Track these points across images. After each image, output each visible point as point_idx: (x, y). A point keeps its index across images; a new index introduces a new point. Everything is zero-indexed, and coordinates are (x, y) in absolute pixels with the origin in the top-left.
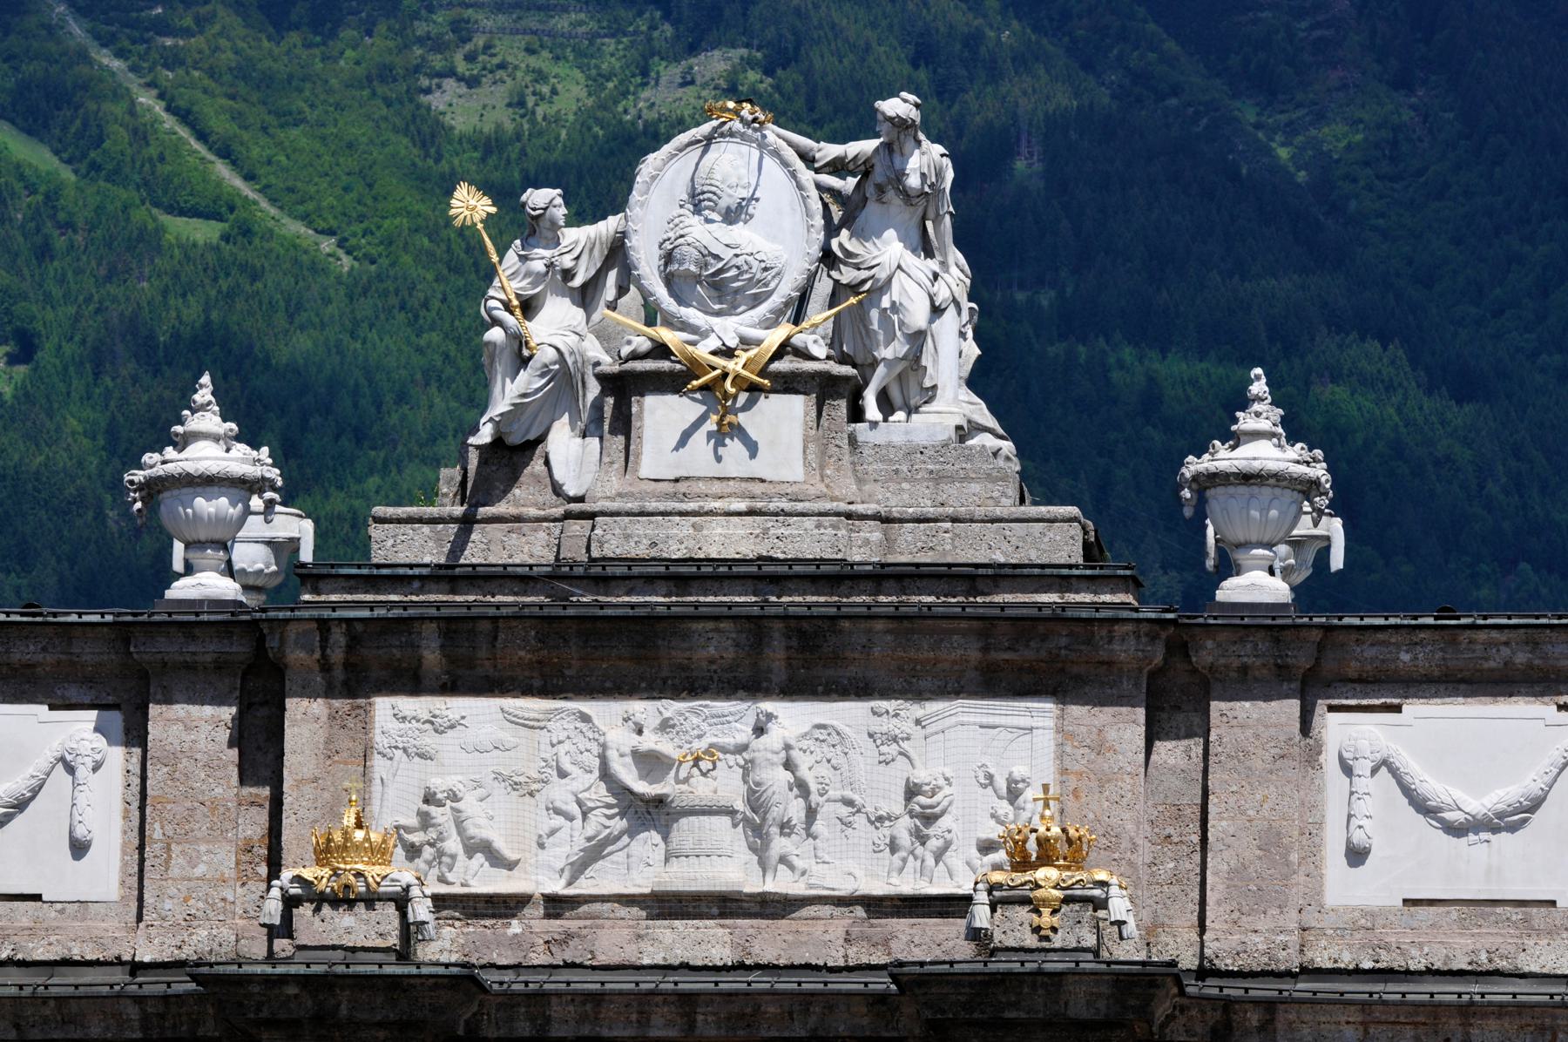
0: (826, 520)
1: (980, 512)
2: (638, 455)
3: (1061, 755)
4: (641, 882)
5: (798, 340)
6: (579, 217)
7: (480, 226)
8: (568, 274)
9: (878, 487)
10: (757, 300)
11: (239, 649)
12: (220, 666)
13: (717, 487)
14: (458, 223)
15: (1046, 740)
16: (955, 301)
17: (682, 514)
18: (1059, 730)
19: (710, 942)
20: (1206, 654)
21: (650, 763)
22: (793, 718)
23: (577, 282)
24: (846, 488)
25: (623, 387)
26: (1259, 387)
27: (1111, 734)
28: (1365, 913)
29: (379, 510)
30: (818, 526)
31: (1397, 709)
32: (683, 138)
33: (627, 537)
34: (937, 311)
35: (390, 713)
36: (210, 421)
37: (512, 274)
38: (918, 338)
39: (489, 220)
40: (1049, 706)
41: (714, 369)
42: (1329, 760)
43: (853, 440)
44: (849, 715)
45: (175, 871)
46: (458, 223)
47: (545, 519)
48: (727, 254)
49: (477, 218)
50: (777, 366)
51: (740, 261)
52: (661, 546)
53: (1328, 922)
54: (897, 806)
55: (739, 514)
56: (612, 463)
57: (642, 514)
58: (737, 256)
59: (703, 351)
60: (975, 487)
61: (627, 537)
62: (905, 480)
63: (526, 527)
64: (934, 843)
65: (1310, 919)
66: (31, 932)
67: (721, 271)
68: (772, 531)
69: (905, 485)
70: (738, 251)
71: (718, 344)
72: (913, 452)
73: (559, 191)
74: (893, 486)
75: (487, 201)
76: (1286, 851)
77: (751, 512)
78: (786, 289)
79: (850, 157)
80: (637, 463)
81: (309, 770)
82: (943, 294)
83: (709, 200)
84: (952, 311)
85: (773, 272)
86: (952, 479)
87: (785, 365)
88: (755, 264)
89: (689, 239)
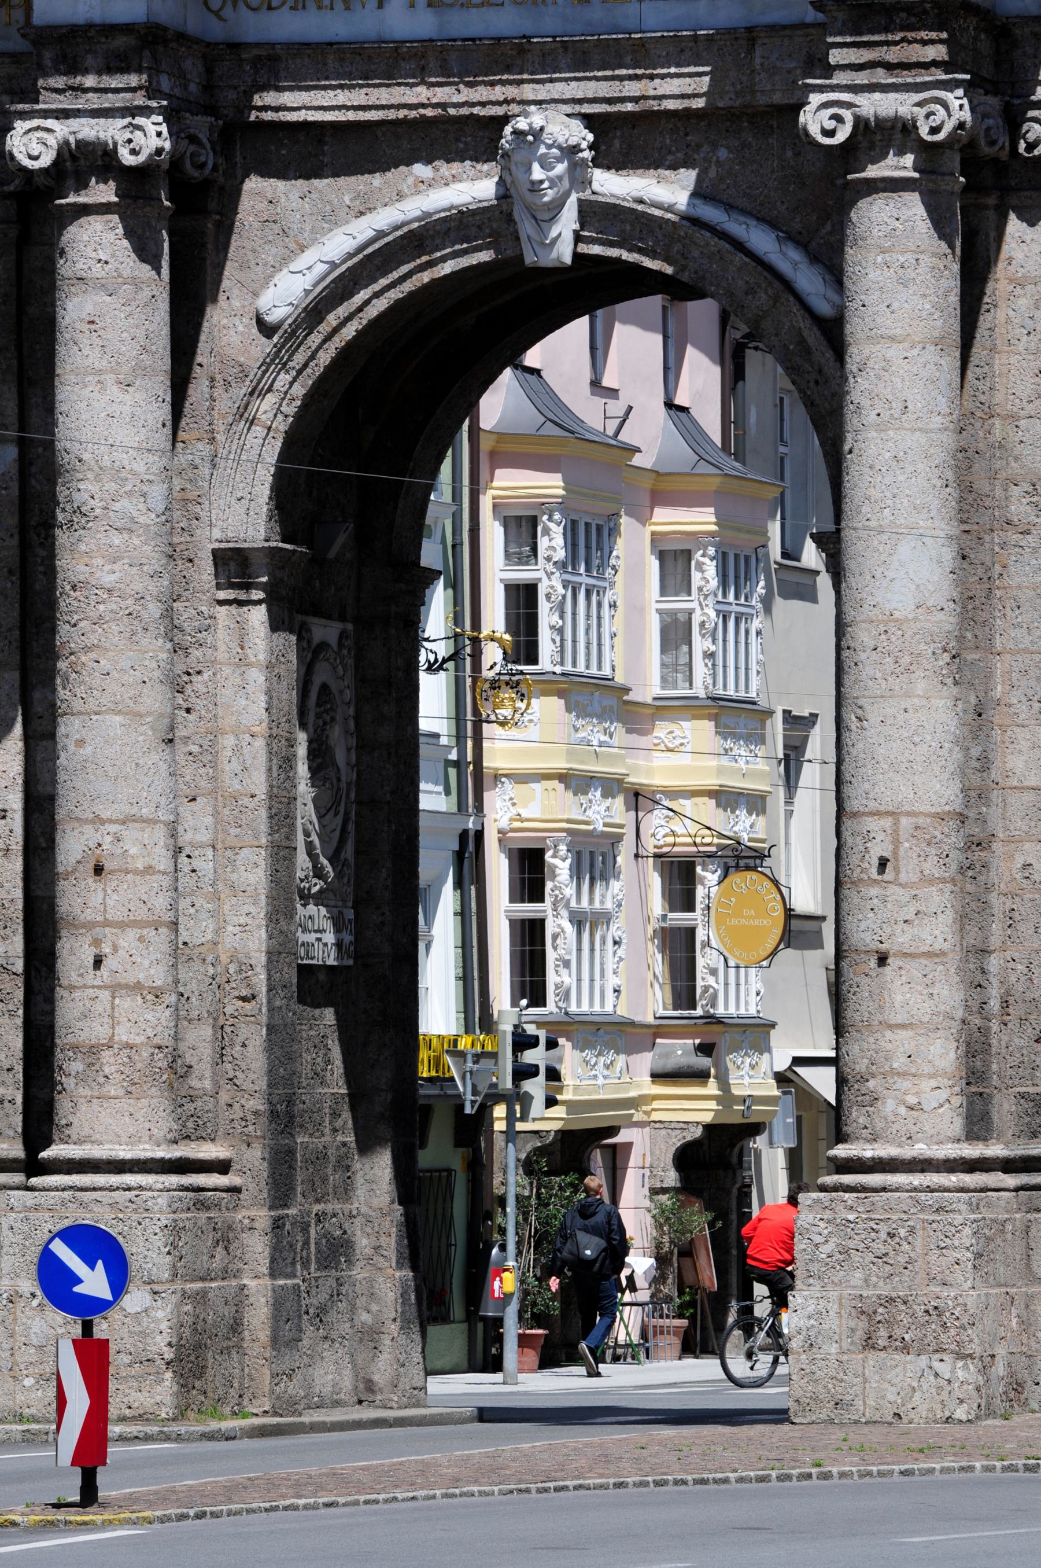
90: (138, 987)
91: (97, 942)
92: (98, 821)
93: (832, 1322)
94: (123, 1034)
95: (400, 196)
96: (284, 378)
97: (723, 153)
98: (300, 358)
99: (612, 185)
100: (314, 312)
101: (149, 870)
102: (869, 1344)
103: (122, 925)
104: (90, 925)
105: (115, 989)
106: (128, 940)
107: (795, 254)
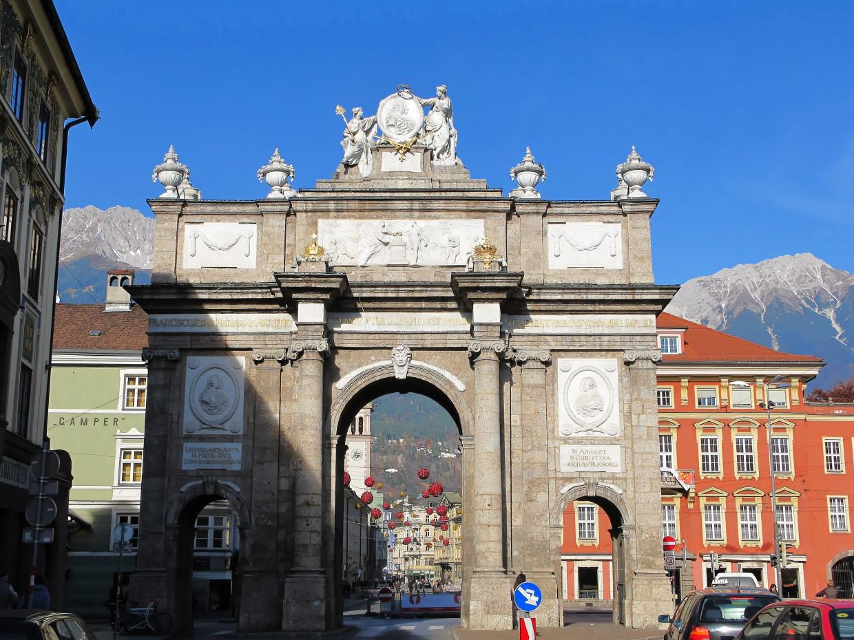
3: (486, 233)
4: (385, 263)
10: (409, 131)
11: (286, 208)
12: (281, 213)
13: (400, 174)
15: (482, 229)
18: (485, 227)
19: (400, 277)
20: (519, 209)
21: (386, 233)
22: (422, 223)
23: (365, 130)
25: (377, 149)
26: (528, 151)
27: (498, 228)
28: (559, 270)
29: (318, 180)
31: (565, 223)
32: (392, 95)
33: (379, 184)
35: (321, 223)
36: (278, 158)
40: (482, 221)
42: (549, 234)
43: (432, 165)
44: (435, 223)
45: (269, 261)
53: (550, 273)
54: (446, 243)
60: (461, 175)
64: (456, 254)
65: (545, 272)
66: (235, 275)
72: (445, 167)
76: (540, 256)
81: (302, 237)
86: (455, 173)
90: (316, 531)
91: (307, 521)
92: (308, 494)
93: (480, 608)
94: (313, 542)
95: (368, 364)
96: (341, 401)
97: (438, 357)
98: (345, 397)
99: (413, 362)
100: (350, 385)
101: (318, 505)
102: (488, 613)
103: (313, 517)
104: (305, 517)
105: (311, 531)
106: (314, 521)
107: (455, 377)
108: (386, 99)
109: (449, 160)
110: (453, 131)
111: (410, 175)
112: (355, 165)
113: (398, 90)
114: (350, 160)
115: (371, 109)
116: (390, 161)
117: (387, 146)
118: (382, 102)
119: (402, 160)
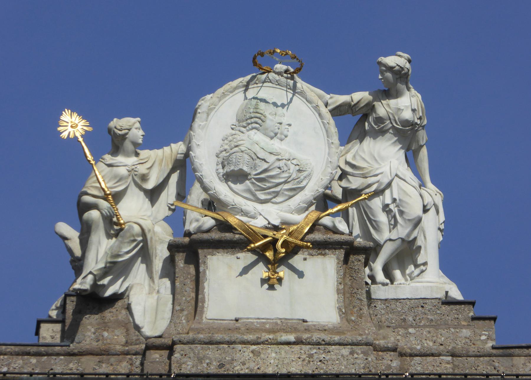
0: (357, 349)
1: (473, 349)
2: (204, 301)
5: (327, 221)
6: (153, 141)
7: (81, 139)
8: (144, 178)
9: (389, 331)
14: (64, 135)
16: (435, 205)
17: (243, 343)
24: (368, 331)
30: (352, 353)
34: (425, 210)
37: (104, 175)
38: (417, 222)
39: (86, 136)
41: (265, 237)
46: (64, 135)
47: (127, 353)
48: (271, 159)
49: (78, 135)
50: (311, 237)
51: (281, 164)
52: (228, 366)
55: (288, 343)
56: (182, 310)
57: (211, 343)
58: (279, 160)
59: (258, 223)
61: (200, 360)
62: (411, 326)
63: (113, 359)
67: (265, 171)
68: (316, 356)
69: (411, 330)
70: (280, 157)
71: (265, 223)
73: (139, 119)
74: (402, 331)
75: (83, 122)
77: (299, 342)
78: (312, 188)
79: (355, 101)
80: (202, 312)
82: (428, 200)
83: (256, 123)
84: (433, 211)
85: (305, 174)
87: (318, 236)
88: (292, 167)
89: (243, 148)
108: (220, 91)
109: (430, 281)
110: (433, 194)
111: (302, 335)
112: (116, 297)
113: (258, 64)
114: (106, 281)
115: (172, 122)
116: (231, 289)
117: (230, 238)
118: (206, 102)
119: (271, 284)
